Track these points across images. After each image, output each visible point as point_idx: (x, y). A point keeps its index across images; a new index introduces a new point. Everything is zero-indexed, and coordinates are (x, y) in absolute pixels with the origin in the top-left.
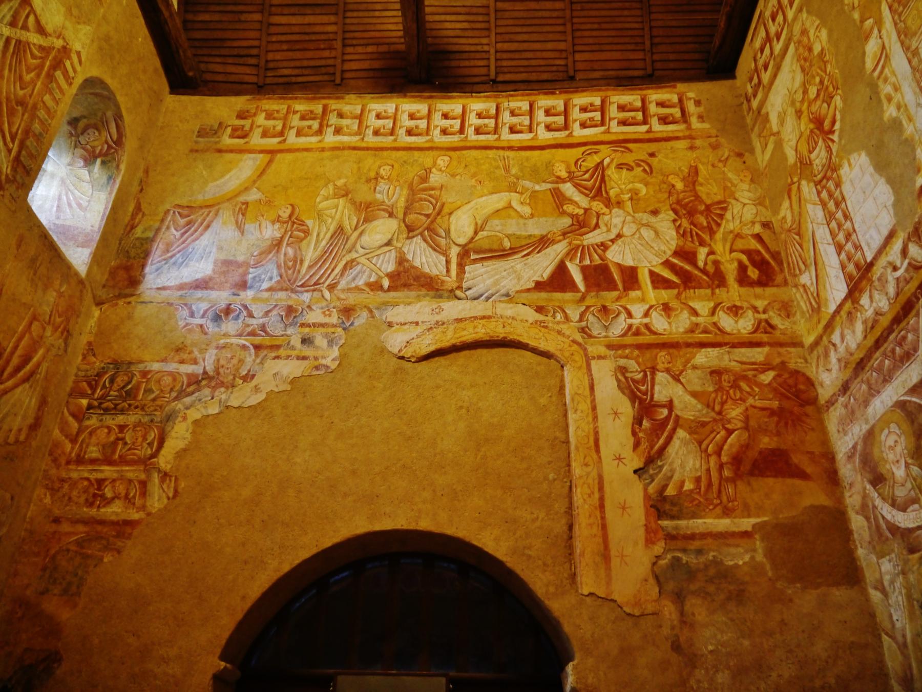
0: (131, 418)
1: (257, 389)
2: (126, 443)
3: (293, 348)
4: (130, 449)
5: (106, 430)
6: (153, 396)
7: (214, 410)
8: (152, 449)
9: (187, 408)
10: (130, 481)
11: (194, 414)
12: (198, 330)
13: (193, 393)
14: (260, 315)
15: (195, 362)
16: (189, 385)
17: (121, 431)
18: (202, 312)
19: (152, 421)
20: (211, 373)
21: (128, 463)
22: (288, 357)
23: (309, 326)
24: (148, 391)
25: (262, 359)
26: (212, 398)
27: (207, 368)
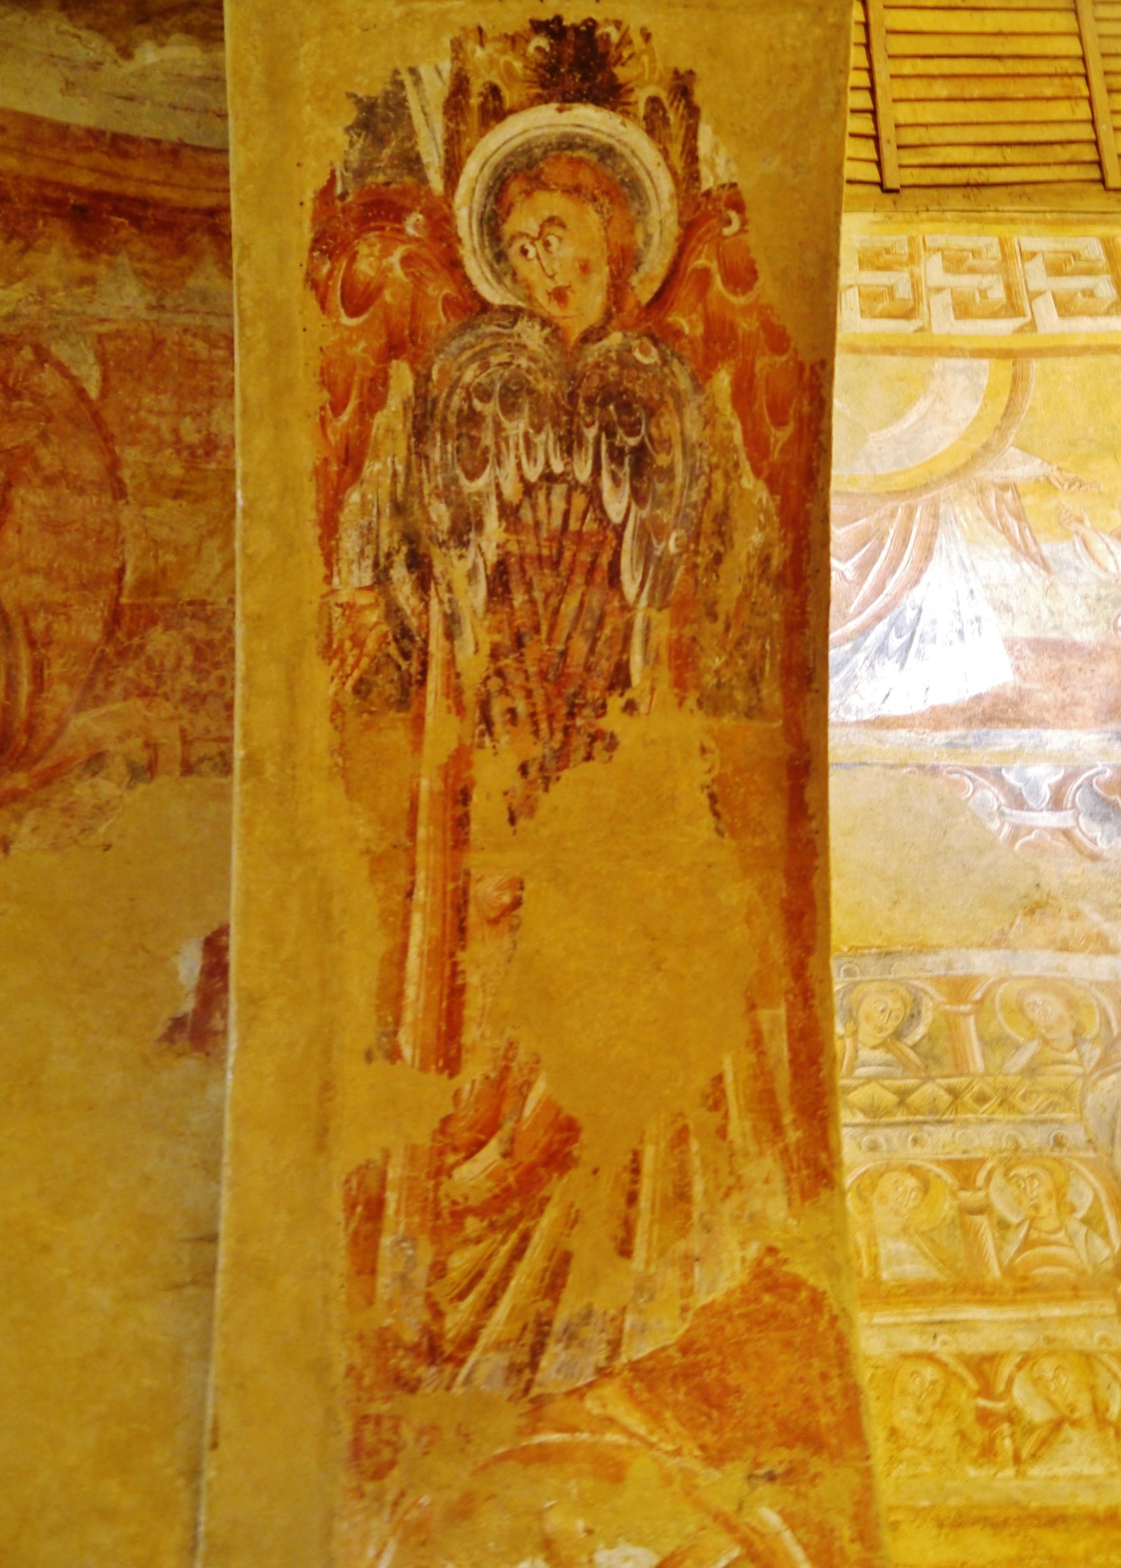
2: (1003, 1226)
4: (1027, 1244)
5: (911, 1182)
6: (1022, 1059)
8: (1106, 1235)
12: (1061, 844)
17: (967, 1182)
18: (1046, 792)
21: (1048, 1291)
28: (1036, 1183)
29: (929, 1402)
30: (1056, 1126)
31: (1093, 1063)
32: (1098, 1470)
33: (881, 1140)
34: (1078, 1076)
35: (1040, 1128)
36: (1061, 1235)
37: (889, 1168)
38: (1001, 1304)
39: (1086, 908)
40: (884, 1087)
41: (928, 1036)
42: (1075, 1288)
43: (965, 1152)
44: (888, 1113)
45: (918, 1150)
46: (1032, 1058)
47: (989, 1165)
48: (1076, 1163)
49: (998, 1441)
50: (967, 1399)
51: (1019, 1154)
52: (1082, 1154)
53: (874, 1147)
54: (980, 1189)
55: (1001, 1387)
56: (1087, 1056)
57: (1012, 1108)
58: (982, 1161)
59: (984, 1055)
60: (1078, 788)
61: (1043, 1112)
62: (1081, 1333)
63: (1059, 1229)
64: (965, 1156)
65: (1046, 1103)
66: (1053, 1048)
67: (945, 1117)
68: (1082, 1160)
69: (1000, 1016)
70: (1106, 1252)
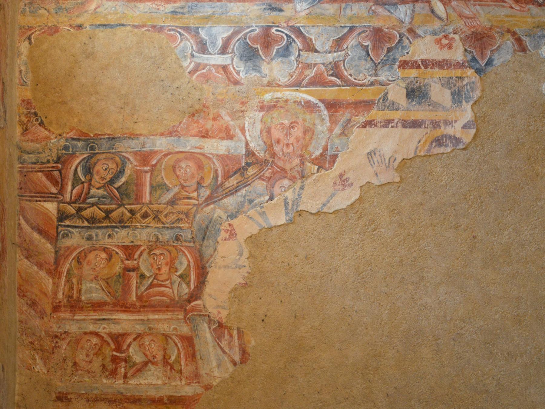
0: (142, 235)
1: (343, 181)
2: (142, 276)
3: (394, 106)
4: (151, 286)
5: (104, 255)
6: (168, 196)
7: (279, 218)
8: (188, 284)
9: (232, 216)
10: (166, 337)
11: (246, 227)
12: (220, 75)
13: (236, 190)
14: (327, 47)
15: (230, 137)
16: (227, 176)
17: (129, 257)
18: (220, 43)
19: (177, 239)
20: (261, 154)
21: (156, 308)
22: (387, 123)
23: (415, 65)
24: (158, 187)
25: (345, 127)
26: (271, 199)
27: (252, 145)
28: (162, 258)
29: (92, 353)
30: (178, 230)
31: (204, 199)
32: (160, 382)
33: (94, 235)
34: (195, 205)
35: (170, 231)
36: (167, 282)
37: (93, 249)
38: (133, 312)
39: (223, 113)
40: (100, 209)
41: (126, 183)
42: (168, 307)
43: (132, 242)
44: (100, 222)
45: (110, 240)
46: (174, 195)
47: (142, 248)
48: (182, 248)
49: (119, 369)
50: (108, 352)
51: (158, 244)
52: (187, 244)
53: (90, 238)
54: (136, 260)
55: (125, 347)
56: (202, 195)
57: (159, 220)
58: (140, 246)
59: (151, 193)
60: (238, 40)
61: (173, 223)
62: (166, 326)
63: (167, 280)
64: (132, 244)
65: (177, 218)
66: (185, 191)
67: (126, 225)
68: (186, 247)
69: (163, 174)
70: (187, 291)
